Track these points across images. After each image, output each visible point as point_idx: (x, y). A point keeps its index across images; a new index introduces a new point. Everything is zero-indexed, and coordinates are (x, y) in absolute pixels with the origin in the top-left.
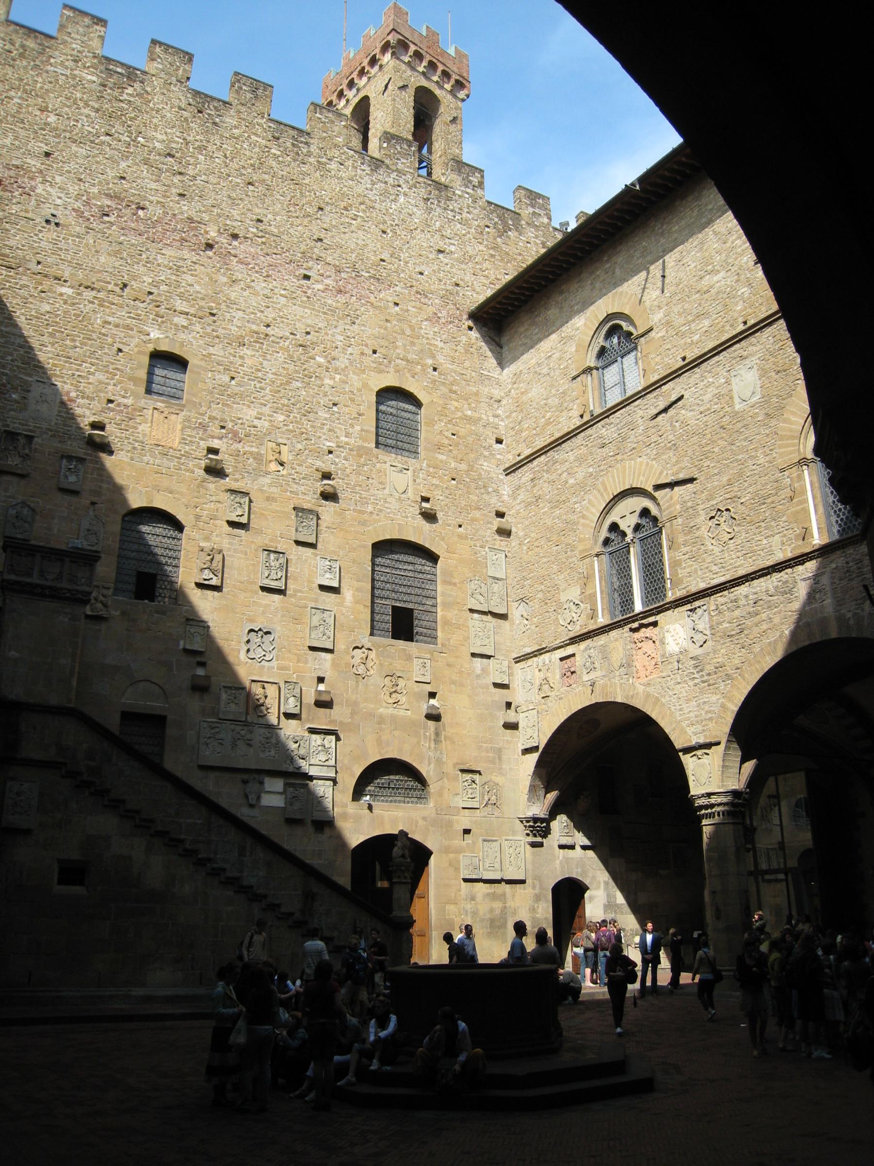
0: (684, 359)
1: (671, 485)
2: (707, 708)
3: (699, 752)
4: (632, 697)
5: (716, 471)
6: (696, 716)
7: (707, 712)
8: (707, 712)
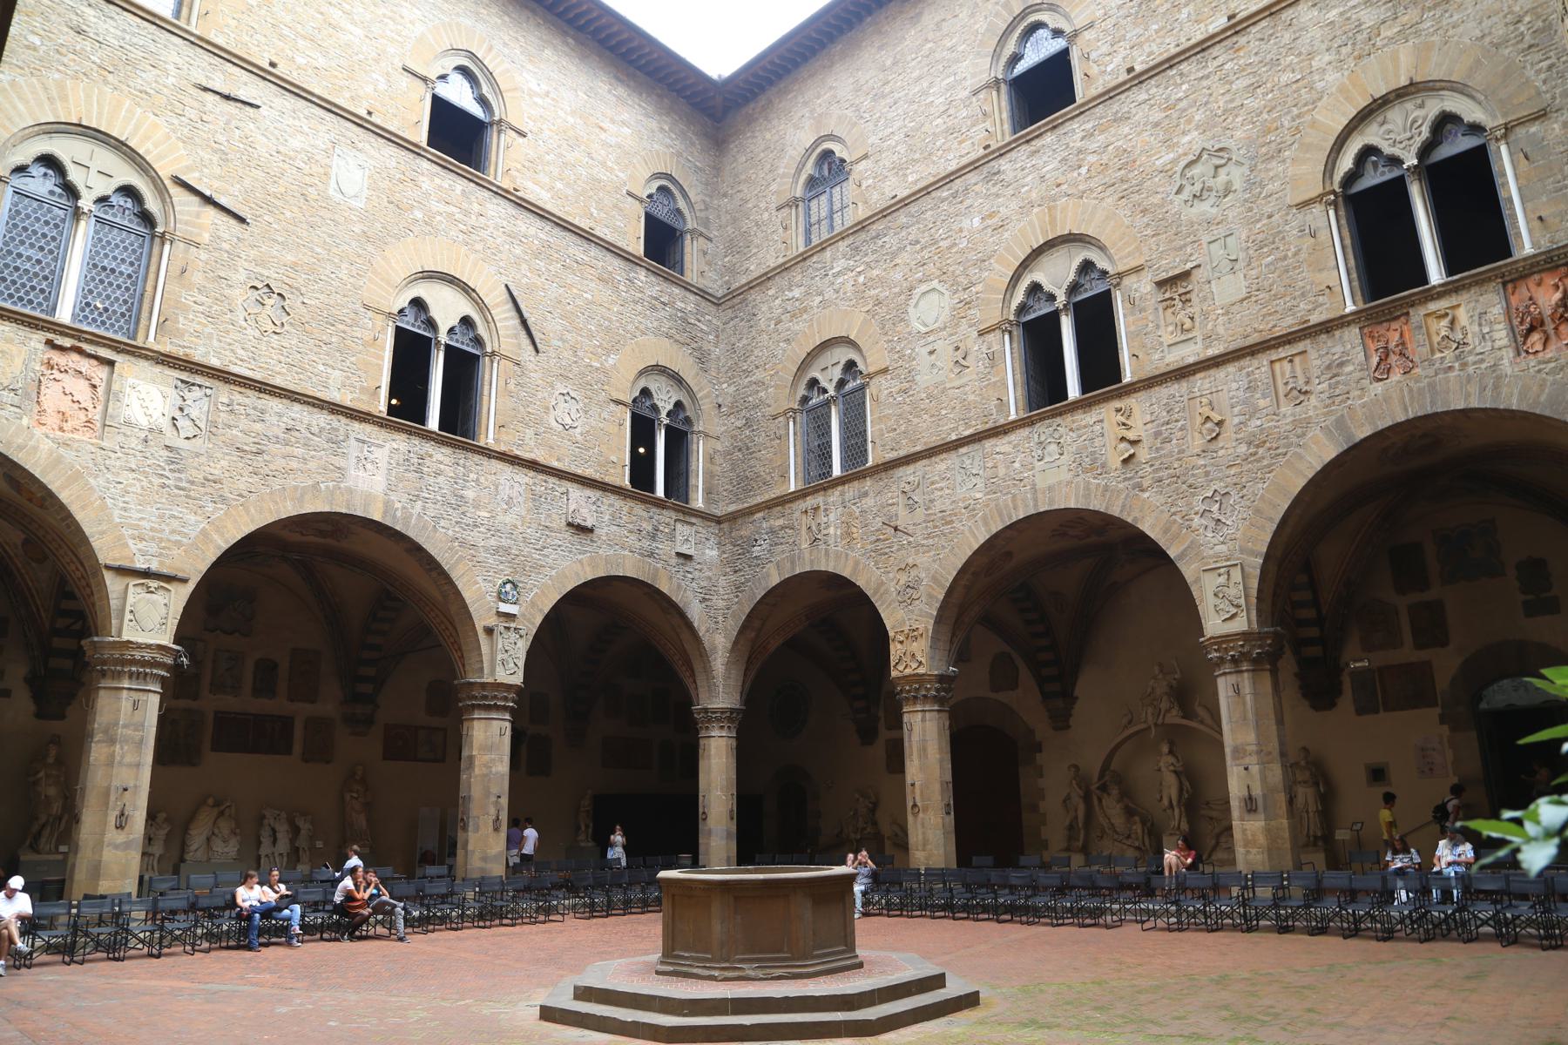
0: (273, 65)
1: (208, 200)
2: (175, 524)
3: (153, 584)
4: (20, 448)
5: (280, 239)
6: (152, 529)
7: (173, 532)
8: (173, 532)
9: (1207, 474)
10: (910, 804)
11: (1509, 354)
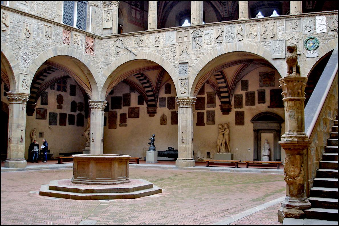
9: (25, 46)
10: (8, 138)
11: (84, 51)
